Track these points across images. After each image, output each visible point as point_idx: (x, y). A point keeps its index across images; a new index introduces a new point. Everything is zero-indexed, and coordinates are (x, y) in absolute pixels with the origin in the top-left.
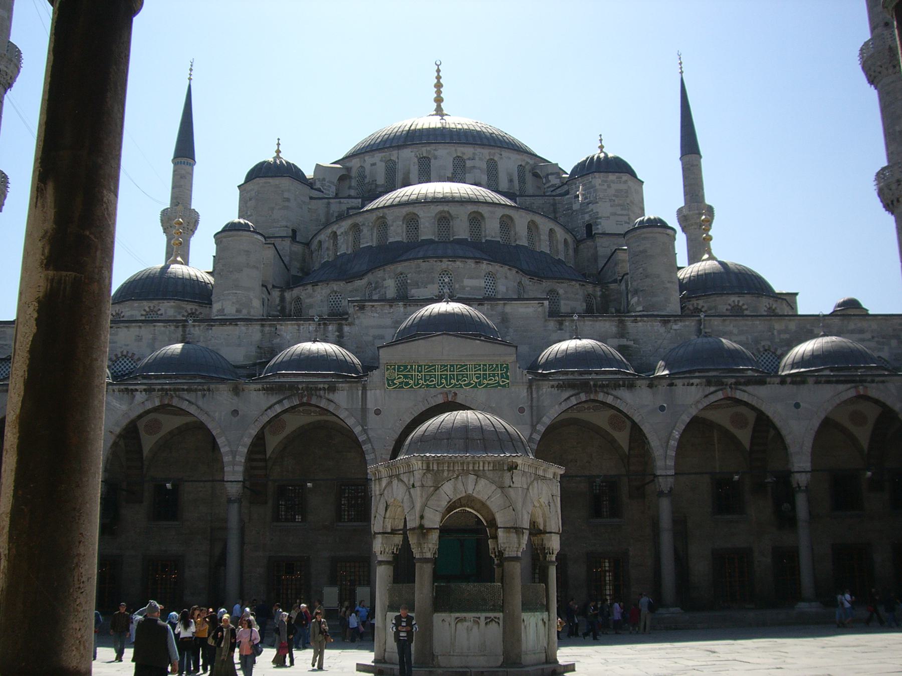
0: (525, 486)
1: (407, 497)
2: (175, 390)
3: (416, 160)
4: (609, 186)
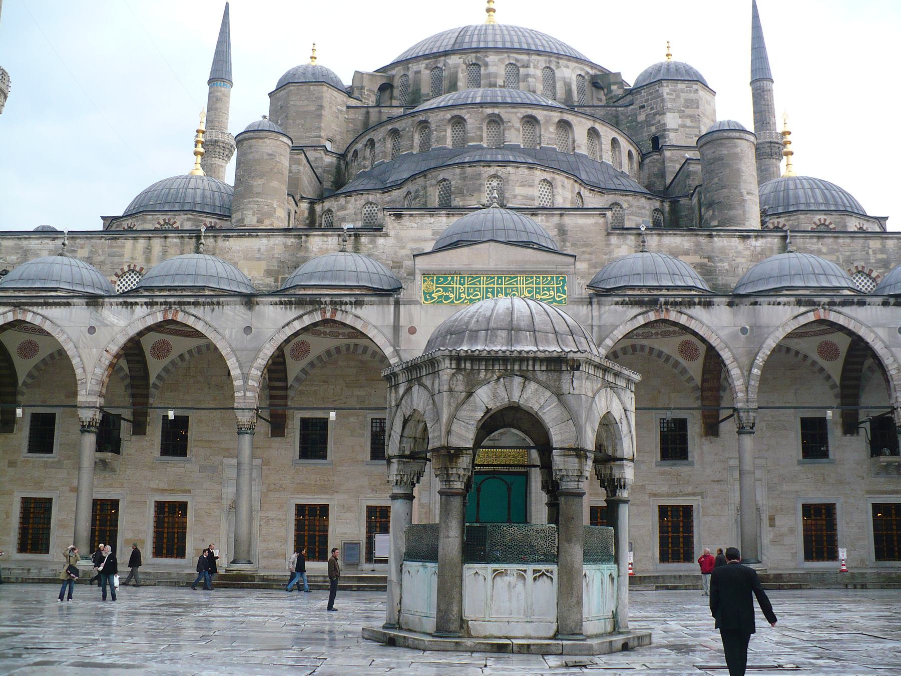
0: (590, 394)
2: (180, 304)
3: (464, 66)
4: (678, 96)
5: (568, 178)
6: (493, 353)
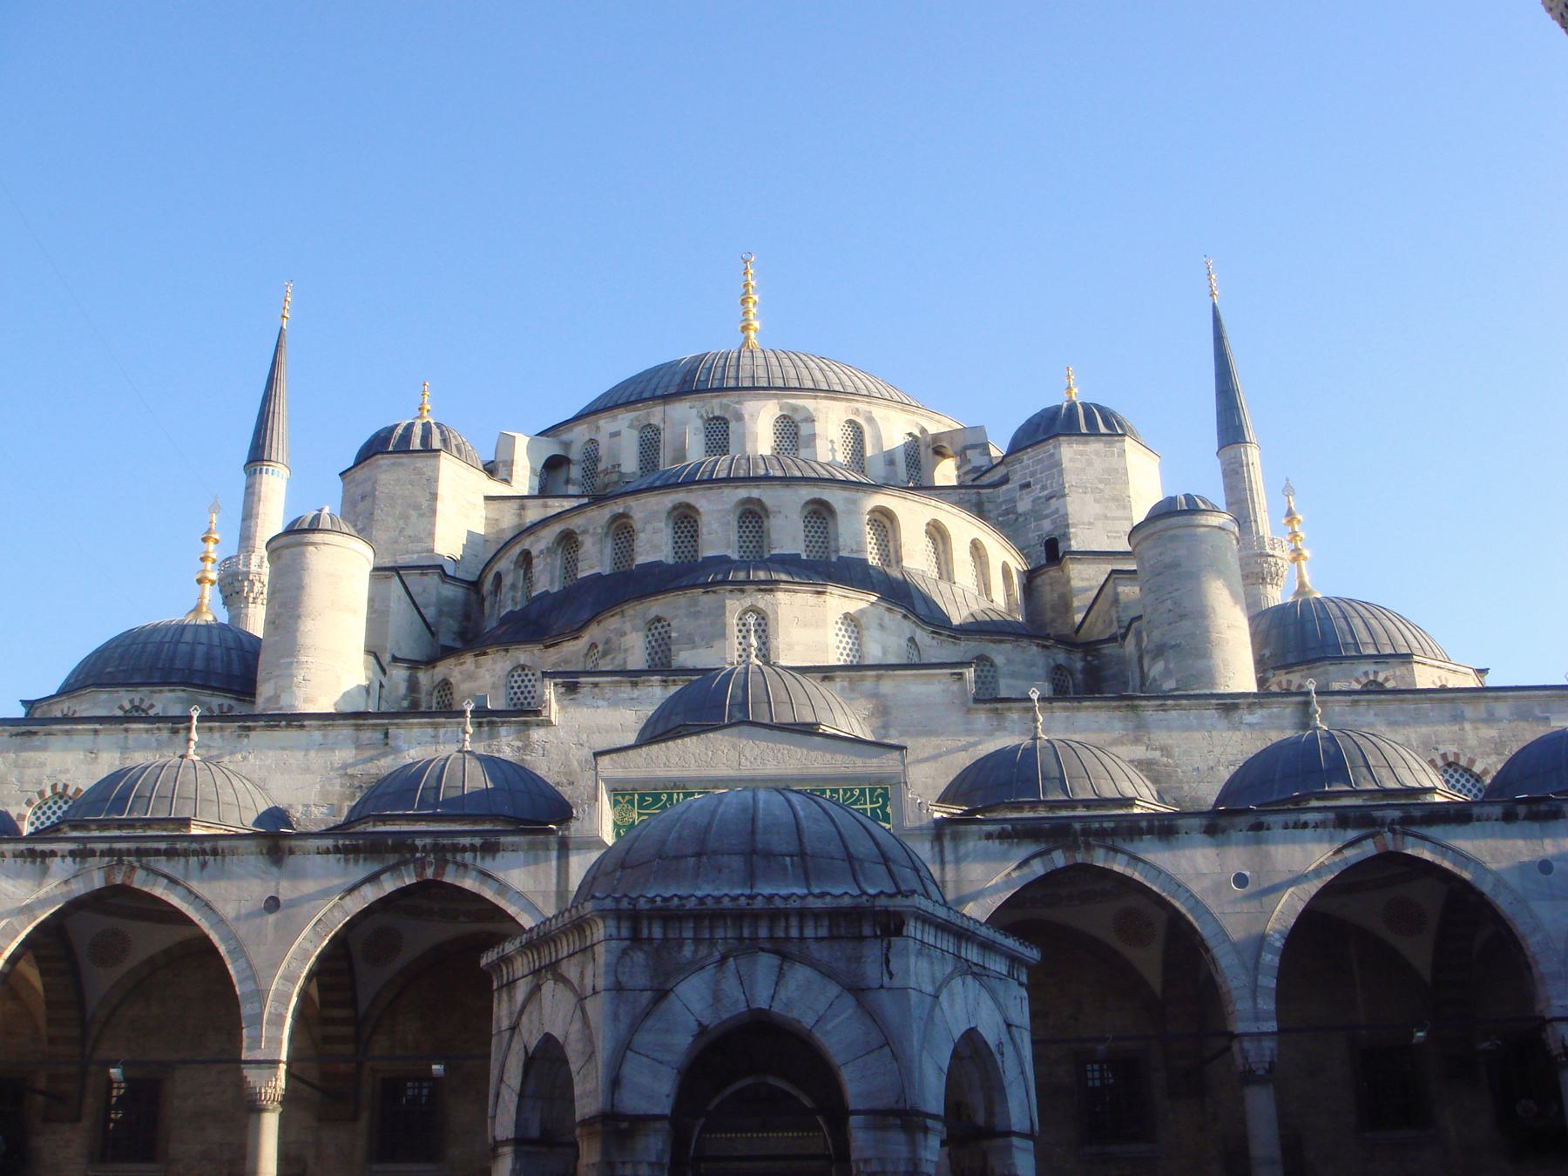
0: (929, 989)
1: (577, 1026)
2: (140, 853)
3: (699, 423)
4: (1090, 463)
5: (889, 610)
6: (710, 902)
